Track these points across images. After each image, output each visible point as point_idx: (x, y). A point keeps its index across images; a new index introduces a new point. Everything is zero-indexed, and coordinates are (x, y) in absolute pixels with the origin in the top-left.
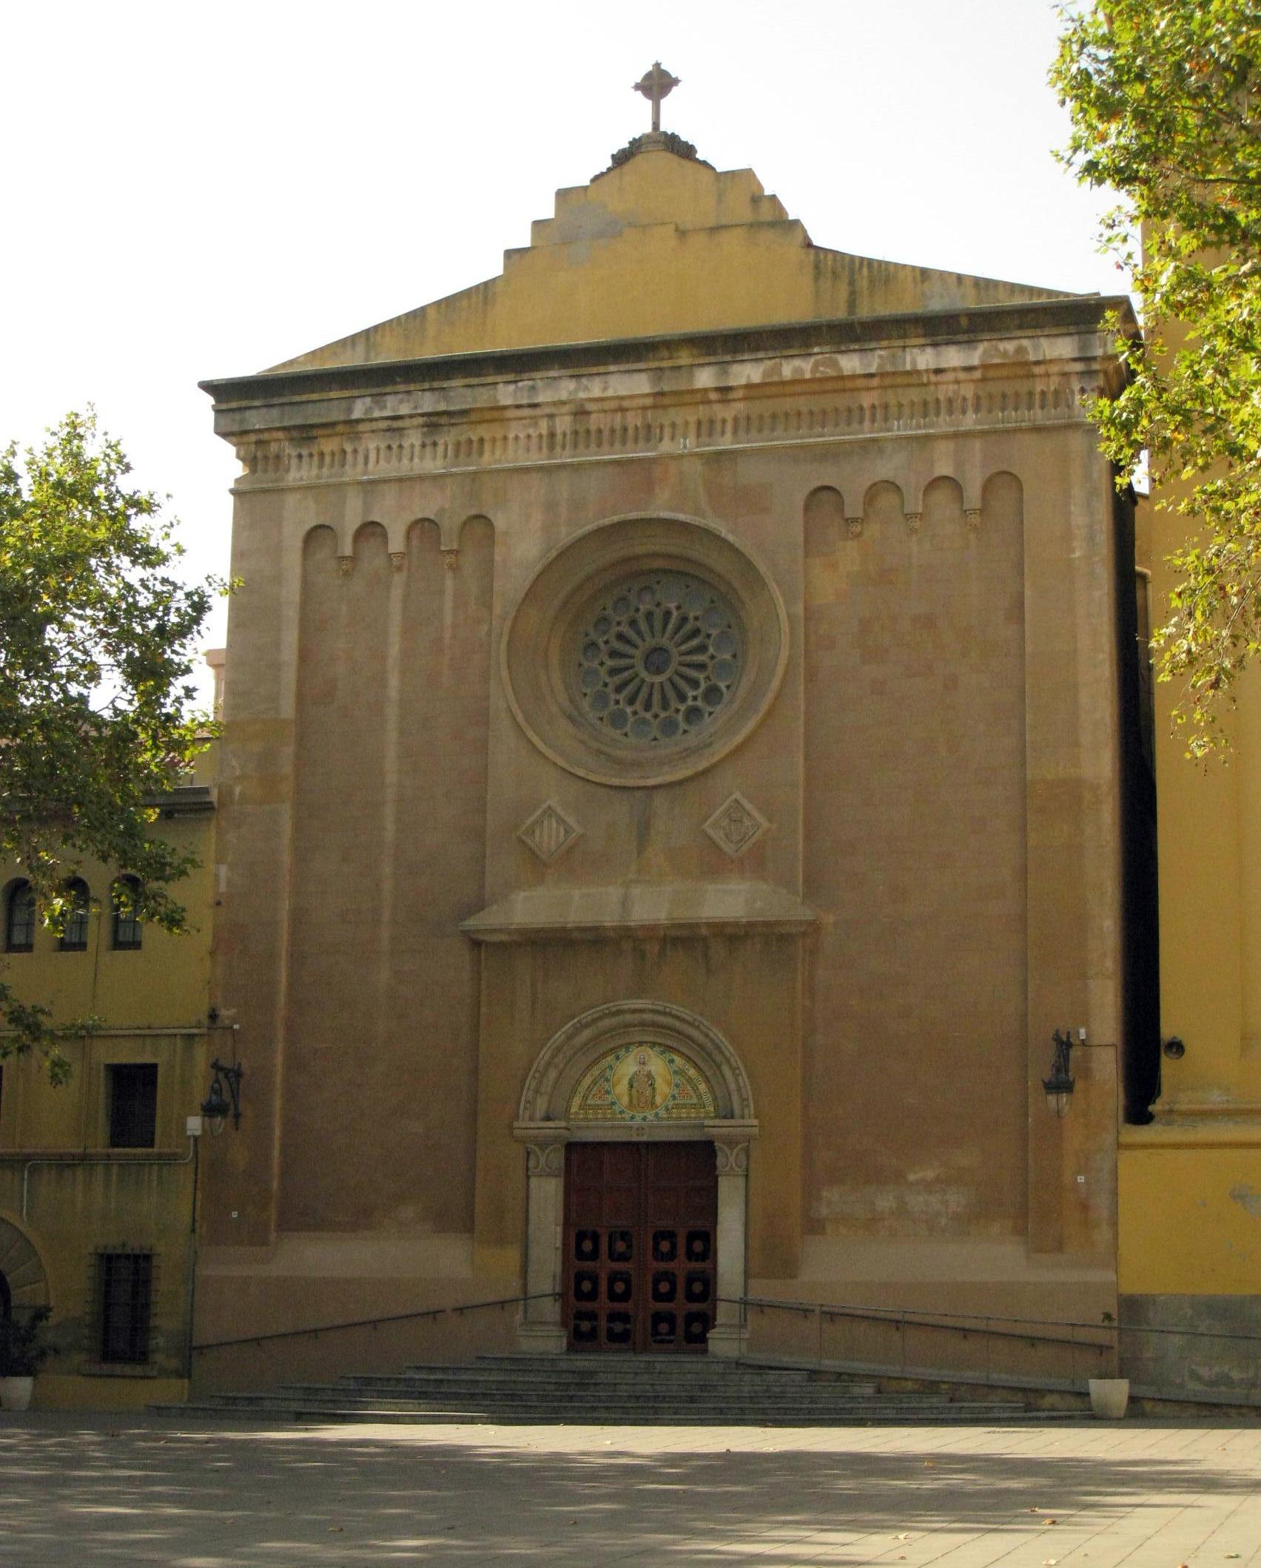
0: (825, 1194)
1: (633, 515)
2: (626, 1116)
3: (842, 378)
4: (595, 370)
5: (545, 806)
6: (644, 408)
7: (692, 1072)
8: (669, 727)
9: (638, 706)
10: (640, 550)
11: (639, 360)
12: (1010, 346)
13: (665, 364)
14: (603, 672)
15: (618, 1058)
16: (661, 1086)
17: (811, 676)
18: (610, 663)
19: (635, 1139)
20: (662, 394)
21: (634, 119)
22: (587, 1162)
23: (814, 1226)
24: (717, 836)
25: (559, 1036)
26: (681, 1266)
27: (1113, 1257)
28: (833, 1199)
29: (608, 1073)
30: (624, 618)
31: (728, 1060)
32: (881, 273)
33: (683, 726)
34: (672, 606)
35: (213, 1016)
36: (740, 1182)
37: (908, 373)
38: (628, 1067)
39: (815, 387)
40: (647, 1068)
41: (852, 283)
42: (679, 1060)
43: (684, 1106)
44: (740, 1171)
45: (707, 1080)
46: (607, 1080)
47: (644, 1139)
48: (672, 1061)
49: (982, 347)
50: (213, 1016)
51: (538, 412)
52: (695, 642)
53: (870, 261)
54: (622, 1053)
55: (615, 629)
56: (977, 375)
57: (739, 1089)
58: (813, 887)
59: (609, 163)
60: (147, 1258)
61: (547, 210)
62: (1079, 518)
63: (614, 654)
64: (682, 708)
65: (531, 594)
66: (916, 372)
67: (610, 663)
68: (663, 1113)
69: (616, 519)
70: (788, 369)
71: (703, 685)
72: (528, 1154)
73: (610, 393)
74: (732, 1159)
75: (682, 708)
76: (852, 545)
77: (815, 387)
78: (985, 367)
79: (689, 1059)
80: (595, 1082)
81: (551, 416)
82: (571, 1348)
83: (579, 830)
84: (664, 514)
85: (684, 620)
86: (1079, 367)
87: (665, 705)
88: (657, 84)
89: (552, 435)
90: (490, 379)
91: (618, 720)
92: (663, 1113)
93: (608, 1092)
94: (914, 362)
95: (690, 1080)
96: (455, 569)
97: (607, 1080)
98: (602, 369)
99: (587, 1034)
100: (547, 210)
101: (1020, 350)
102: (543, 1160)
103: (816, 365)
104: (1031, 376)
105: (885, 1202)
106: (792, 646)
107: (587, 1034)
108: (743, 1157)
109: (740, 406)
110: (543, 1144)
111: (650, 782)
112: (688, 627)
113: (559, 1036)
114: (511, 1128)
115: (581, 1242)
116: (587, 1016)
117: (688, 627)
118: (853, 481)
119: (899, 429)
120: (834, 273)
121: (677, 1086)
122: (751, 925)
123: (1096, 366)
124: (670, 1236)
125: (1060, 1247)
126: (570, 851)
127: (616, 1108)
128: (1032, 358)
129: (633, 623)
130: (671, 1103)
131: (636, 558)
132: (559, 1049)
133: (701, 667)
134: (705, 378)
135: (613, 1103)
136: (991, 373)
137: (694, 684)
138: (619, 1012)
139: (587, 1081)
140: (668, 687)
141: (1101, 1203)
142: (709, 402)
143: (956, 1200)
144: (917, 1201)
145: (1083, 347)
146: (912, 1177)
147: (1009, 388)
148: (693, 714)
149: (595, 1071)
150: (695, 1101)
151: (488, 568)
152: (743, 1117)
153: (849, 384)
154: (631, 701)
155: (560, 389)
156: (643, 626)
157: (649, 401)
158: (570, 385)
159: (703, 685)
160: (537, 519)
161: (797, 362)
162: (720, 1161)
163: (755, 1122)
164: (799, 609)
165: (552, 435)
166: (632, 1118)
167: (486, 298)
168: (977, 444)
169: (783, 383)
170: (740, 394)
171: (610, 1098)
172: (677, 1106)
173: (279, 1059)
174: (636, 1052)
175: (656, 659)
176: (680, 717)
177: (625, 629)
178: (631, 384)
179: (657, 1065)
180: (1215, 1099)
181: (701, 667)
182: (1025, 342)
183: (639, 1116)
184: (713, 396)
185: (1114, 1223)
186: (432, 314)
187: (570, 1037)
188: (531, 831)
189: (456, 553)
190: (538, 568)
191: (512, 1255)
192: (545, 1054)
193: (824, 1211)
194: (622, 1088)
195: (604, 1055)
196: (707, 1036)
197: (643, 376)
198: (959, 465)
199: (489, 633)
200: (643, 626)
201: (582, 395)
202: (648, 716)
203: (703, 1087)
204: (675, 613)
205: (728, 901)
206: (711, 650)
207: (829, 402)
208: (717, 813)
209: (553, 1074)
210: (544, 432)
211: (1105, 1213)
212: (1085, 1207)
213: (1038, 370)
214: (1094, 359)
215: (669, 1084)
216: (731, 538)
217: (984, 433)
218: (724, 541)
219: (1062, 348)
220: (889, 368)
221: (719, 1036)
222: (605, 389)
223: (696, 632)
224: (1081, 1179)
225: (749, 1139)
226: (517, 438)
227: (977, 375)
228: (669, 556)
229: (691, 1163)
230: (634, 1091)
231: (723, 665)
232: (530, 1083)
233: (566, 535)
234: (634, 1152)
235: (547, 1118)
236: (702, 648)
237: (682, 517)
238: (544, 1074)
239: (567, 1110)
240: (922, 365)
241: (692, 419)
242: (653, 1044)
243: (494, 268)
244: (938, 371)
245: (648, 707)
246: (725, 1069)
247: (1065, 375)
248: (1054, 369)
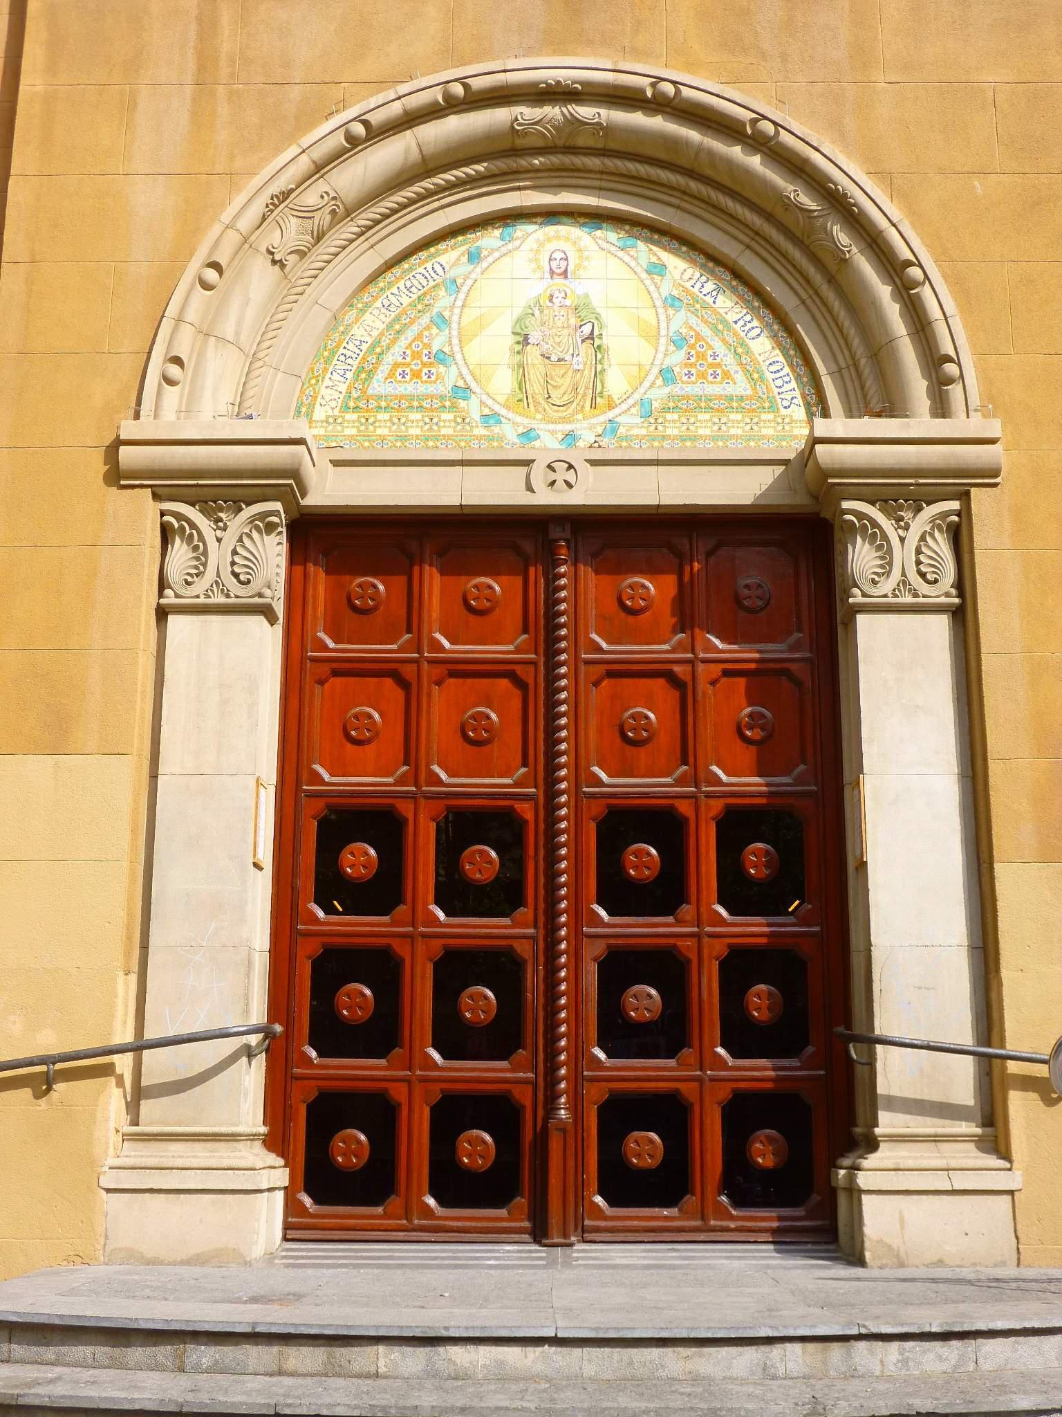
2: (509, 432)
15: (474, 257)
19: (544, 497)
25: (287, 164)
29: (443, 301)
40: (578, 288)
44: (943, 591)
46: (442, 321)
48: (658, 269)
54: (489, 239)
68: (631, 422)
72: (166, 534)
74: (903, 556)
80: (396, 328)
92: (631, 422)
93: (441, 358)
95: (719, 325)
97: (442, 321)
102: (218, 555)
108: (942, 546)
110: (219, 492)
115: (335, 847)
121: (679, 341)
124: (661, 824)
127: (473, 408)
130: (659, 394)
135: (462, 391)
150: (741, 386)
162: (861, 558)
166: (528, 435)
171: (450, 376)
172: (677, 404)
174: (530, 234)
192: (242, 207)
203: (763, 347)
215: (652, 336)
225: (960, 484)
230: (532, 354)
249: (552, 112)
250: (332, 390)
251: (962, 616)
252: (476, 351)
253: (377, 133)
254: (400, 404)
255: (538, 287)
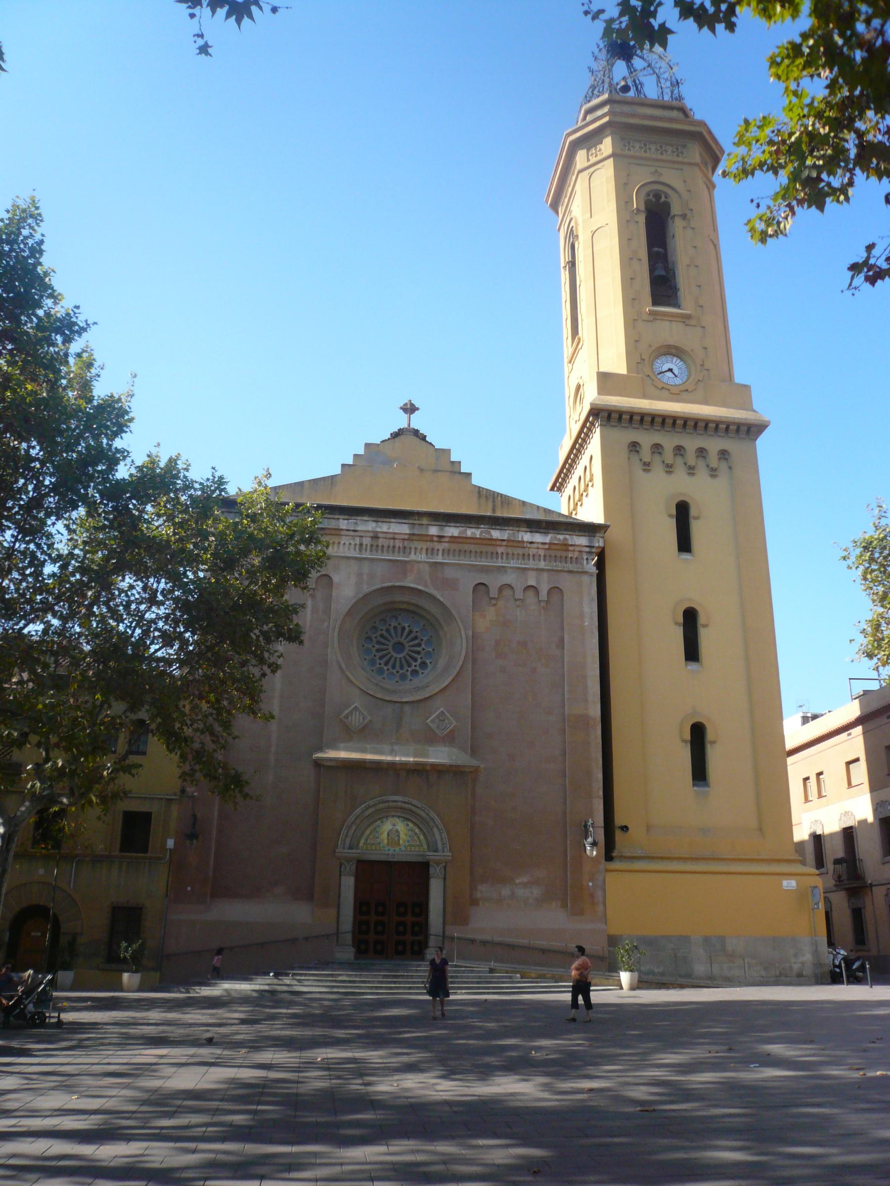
0: (479, 887)
1: (397, 584)
2: (386, 849)
3: (492, 539)
4: (385, 520)
5: (353, 706)
6: (404, 539)
7: (417, 830)
8: (403, 677)
9: (390, 666)
10: (397, 600)
11: (405, 519)
12: (561, 537)
13: (416, 522)
14: (374, 650)
16: (402, 835)
17: (474, 662)
18: (377, 646)
19: (391, 860)
20: (413, 535)
21: (401, 421)
22: (370, 871)
23: (474, 902)
24: (433, 726)
26: (409, 918)
27: (605, 919)
28: (483, 890)
30: (384, 628)
31: (437, 826)
32: (506, 501)
33: (410, 677)
34: (406, 625)
35: (183, 791)
36: (442, 881)
37: (519, 542)
38: (387, 826)
39: (480, 541)
41: (494, 502)
42: (411, 825)
43: (412, 846)
44: (442, 876)
45: (424, 834)
47: (395, 860)
49: (550, 536)
50: (183, 791)
51: (356, 534)
52: (416, 642)
53: (502, 495)
55: (379, 632)
56: (547, 547)
57: (442, 839)
58: (474, 751)
59: (389, 436)
60: (141, 909)
61: (361, 451)
62: (586, 610)
63: (378, 643)
64: (410, 669)
65: (349, 613)
66: (523, 542)
67: (377, 646)
68: (403, 848)
69: (390, 584)
70: (469, 533)
71: (419, 661)
73: (391, 531)
74: (438, 870)
75: (410, 669)
76: (492, 609)
77: (480, 541)
78: (550, 544)
79: (415, 824)
80: (371, 832)
81: (362, 537)
82: (356, 958)
83: (369, 718)
84: (412, 585)
85: (410, 632)
86: (587, 549)
87: (402, 667)
88: (410, 409)
89: (361, 545)
90: (336, 517)
91: (381, 671)
92: (403, 848)
94: (522, 537)
96: (313, 596)
98: (388, 520)
99: (370, 811)
100: (361, 451)
101: (565, 539)
102: (348, 868)
103: (481, 533)
104: (568, 550)
105: (506, 892)
106: (467, 648)
107: (370, 811)
108: (443, 869)
109: (446, 545)
111: (404, 700)
112: (413, 635)
113: (358, 811)
114: (335, 852)
115: (361, 906)
116: (371, 803)
117: (413, 635)
118: (494, 582)
119: (513, 564)
120: (486, 497)
122: (451, 766)
123: (594, 550)
125: (582, 913)
126: (364, 728)
128: (570, 543)
129: (387, 630)
131: (394, 602)
132: (358, 816)
133: (418, 653)
134: (433, 531)
136: (553, 547)
137: (416, 660)
138: (388, 801)
139: (368, 832)
140: (403, 660)
141: (599, 893)
142: (432, 541)
143: (537, 892)
144: (520, 892)
145: (590, 541)
146: (517, 881)
147: (559, 554)
148: (415, 673)
149: (372, 828)
151: (329, 598)
152: (444, 851)
153: (494, 543)
154: (386, 664)
155: (368, 525)
156: (392, 631)
157: (406, 537)
158: (374, 524)
159: (419, 661)
160: (353, 579)
161: (473, 530)
162: (432, 871)
163: (450, 854)
164: (470, 634)
165: (361, 545)
167: (332, 483)
168: (545, 575)
169: (466, 538)
170: (447, 540)
171: (378, 840)
173: (216, 814)
174: (391, 819)
175: (399, 647)
176: (409, 673)
177: (384, 632)
178: (401, 528)
179: (401, 826)
180: (639, 853)
181: (418, 653)
182: (567, 536)
183: (392, 849)
184: (435, 539)
185: (604, 904)
186: (307, 485)
187: (363, 812)
188: (347, 717)
189: (314, 589)
190: (354, 601)
191: (332, 912)
192: (352, 818)
193: (479, 895)
194: (385, 835)
195: (376, 821)
196: (428, 814)
197: (406, 526)
198: (538, 581)
199: (329, 626)
200: (392, 631)
201: (378, 530)
202: (394, 671)
203: (422, 837)
204: (407, 629)
205: (439, 755)
206: (423, 646)
207: (484, 549)
208: (433, 717)
209: (354, 828)
210: (358, 543)
211: (601, 899)
212: (592, 896)
213: (571, 548)
214: (593, 547)
215: (406, 835)
216: (441, 599)
217: (548, 570)
218: (439, 600)
219: (582, 541)
220: (512, 538)
221: (433, 815)
222: (389, 528)
223: (416, 638)
224: (590, 884)
226: (344, 544)
227: (547, 547)
228: (409, 603)
229: (419, 871)
231: (429, 654)
232: (344, 831)
233: (366, 589)
234: (388, 866)
235: (351, 848)
236: (419, 645)
237: (420, 587)
238: (350, 827)
239: (358, 844)
240: (525, 539)
241: (425, 547)
242: (399, 817)
243: (337, 471)
244: (531, 543)
245: (394, 667)
246: (435, 830)
247: (581, 552)
248: (577, 549)
249: (394, 804)
250: (362, 841)
251: (445, 879)
252: (382, 837)
253: (370, 807)
254: (373, 844)
255: (390, 827)
